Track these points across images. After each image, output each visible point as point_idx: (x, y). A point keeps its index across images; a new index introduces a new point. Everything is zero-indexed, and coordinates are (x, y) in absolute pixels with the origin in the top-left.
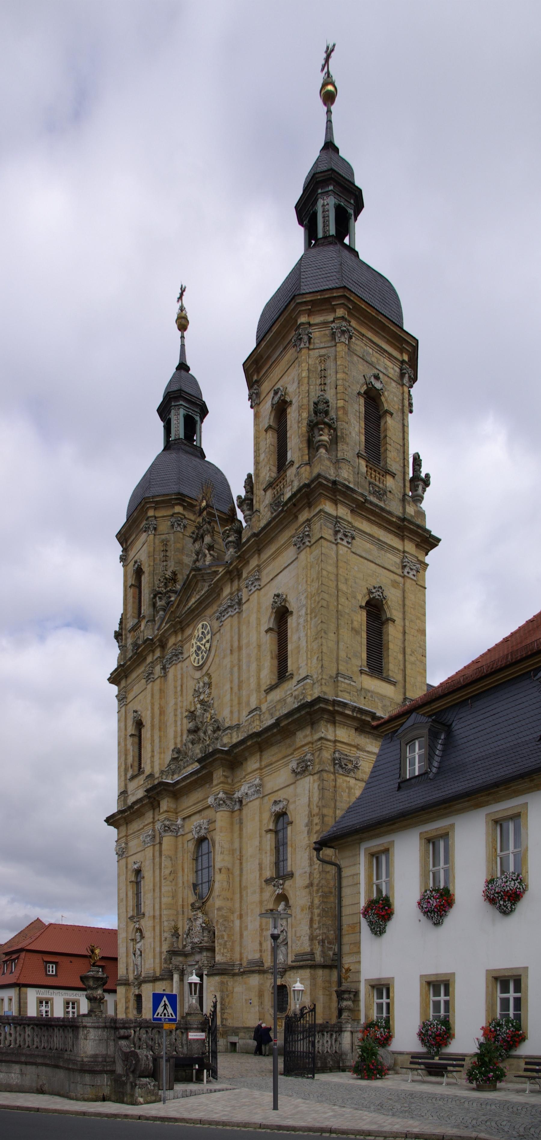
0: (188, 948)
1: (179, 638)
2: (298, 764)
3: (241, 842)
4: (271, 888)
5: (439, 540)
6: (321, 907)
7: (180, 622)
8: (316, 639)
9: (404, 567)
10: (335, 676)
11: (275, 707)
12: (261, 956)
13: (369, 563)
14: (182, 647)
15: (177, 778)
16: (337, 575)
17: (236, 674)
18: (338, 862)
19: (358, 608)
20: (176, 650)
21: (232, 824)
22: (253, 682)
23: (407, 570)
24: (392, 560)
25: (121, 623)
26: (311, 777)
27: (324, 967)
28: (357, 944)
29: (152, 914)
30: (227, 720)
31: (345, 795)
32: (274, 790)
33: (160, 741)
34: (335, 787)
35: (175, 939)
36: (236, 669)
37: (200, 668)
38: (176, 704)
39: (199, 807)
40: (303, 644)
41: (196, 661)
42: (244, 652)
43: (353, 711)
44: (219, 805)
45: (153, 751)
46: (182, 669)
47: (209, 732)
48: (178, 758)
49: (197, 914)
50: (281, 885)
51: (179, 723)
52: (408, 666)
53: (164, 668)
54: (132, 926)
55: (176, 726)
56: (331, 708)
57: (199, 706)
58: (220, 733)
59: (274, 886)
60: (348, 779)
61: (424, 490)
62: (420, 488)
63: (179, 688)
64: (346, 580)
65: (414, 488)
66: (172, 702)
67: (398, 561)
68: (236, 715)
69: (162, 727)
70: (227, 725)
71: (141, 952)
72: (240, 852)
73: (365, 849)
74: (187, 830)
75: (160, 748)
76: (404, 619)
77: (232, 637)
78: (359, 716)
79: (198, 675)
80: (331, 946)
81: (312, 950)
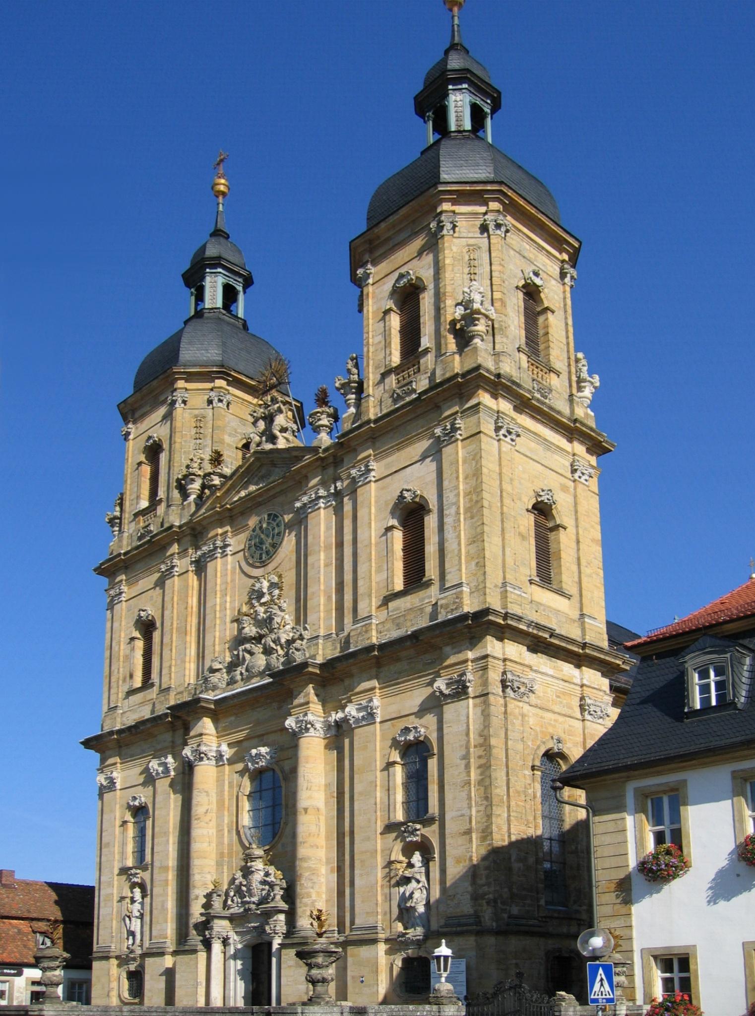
6: (491, 859)
9: (574, 471)
13: (535, 463)
16: (500, 474)
19: (525, 511)
27: (498, 933)
31: (518, 722)
34: (505, 712)
52: (585, 580)
60: (521, 704)
64: (511, 480)
67: (568, 464)
76: (577, 527)
80: (505, 907)
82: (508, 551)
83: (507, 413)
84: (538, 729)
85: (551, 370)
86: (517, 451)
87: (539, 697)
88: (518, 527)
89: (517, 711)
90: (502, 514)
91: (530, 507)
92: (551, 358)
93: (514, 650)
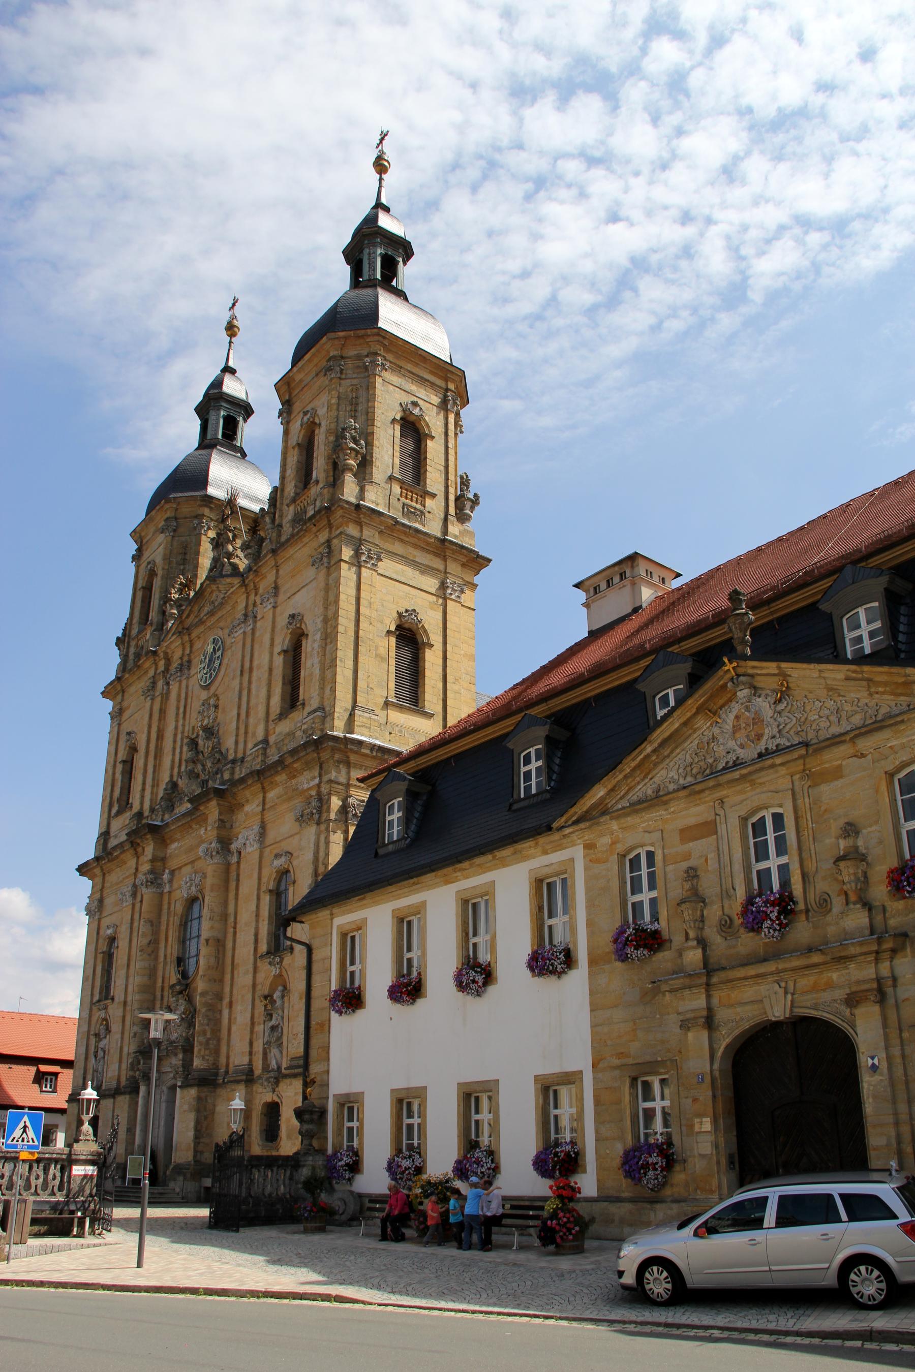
17: (244, 699)
22: (261, 710)
30: (231, 752)
33: (154, 772)
36: (245, 693)
38: (176, 728)
42: (255, 674)
45: (144, 784)
51: (178, 751)
69: (158, 755)
75: (153, 779)
77: (243, 657)
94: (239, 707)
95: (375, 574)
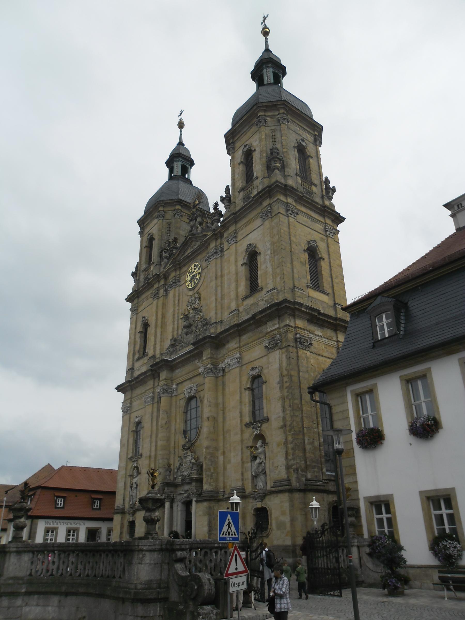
0: (179, 480)
1: (178, 273)
2: (269, 342)
3: (223, 398)
4: (250, 430)
5: (345, 219)
6: (294, 443)
7: (179, 264)
8: (279, 267)
10: (292, 288)
11: (250, 308)
12: (243, 484)
13: (307, 228)
14: (180, 278)
15: (174, 357)
17: (219, 291)
18: (328, 402)
19: (303, 251)
20: (176, 280)
21: (216, 385)
22: (233, 295)
23: (328, 233)
24: (320, 227)
25: (137, 267)
26: (280, 351)
28: (353, 467)
29: (148, 454)
31: (304, 362)
32: (251, 360)
33: (161, 335)
34: (298, 356)
35: (168, 473)
36: (219, 288)
37: (193, 289)
38: (174, 311)
39: (191, 375)
40: (270, 270)
41: (190, 285)
43: (306, 309)
44: (208, 373)
45: (155, 341)
46: (179, 290)
47: (199, 326)
48: (174, 344)
49: (187, 453)
50: (259, 427)
51: (176, 322)
53: (166, 291)
54: (131, 464)
55: (174, 324)
56: (292, 306)
57: (191, 311)
58: (208, 326)
59: (253, 428)
60: (306, 352)
61: (333, 194)
62: (331, 193)
63: (177, 302)
65: (327, 193)
66: (171, 310)
67: (323, 228)
68: (219, 315)
70: (213, 321)
71: (137, 485)
72: (223, 405)
73: (352, 391)
74: (179, 392)
75: (161, 338)
76: (329, 258)
77: (216, 270)
78: (310, 312)
79: (191, 293)
80: (303, 473)
81: (288, 477)
82: (295, 271)
83: (292, 203)
84: (316, 366)
85: (312, 184)
86: (298, 222)
87: (315, 348)
88: (300, 259)
89: (304, 355)
90: (291, 252)
91: (306, 249)
92: (312, 178)
93: (300, 323)
94: (216, 295)
95: (295, 221)
